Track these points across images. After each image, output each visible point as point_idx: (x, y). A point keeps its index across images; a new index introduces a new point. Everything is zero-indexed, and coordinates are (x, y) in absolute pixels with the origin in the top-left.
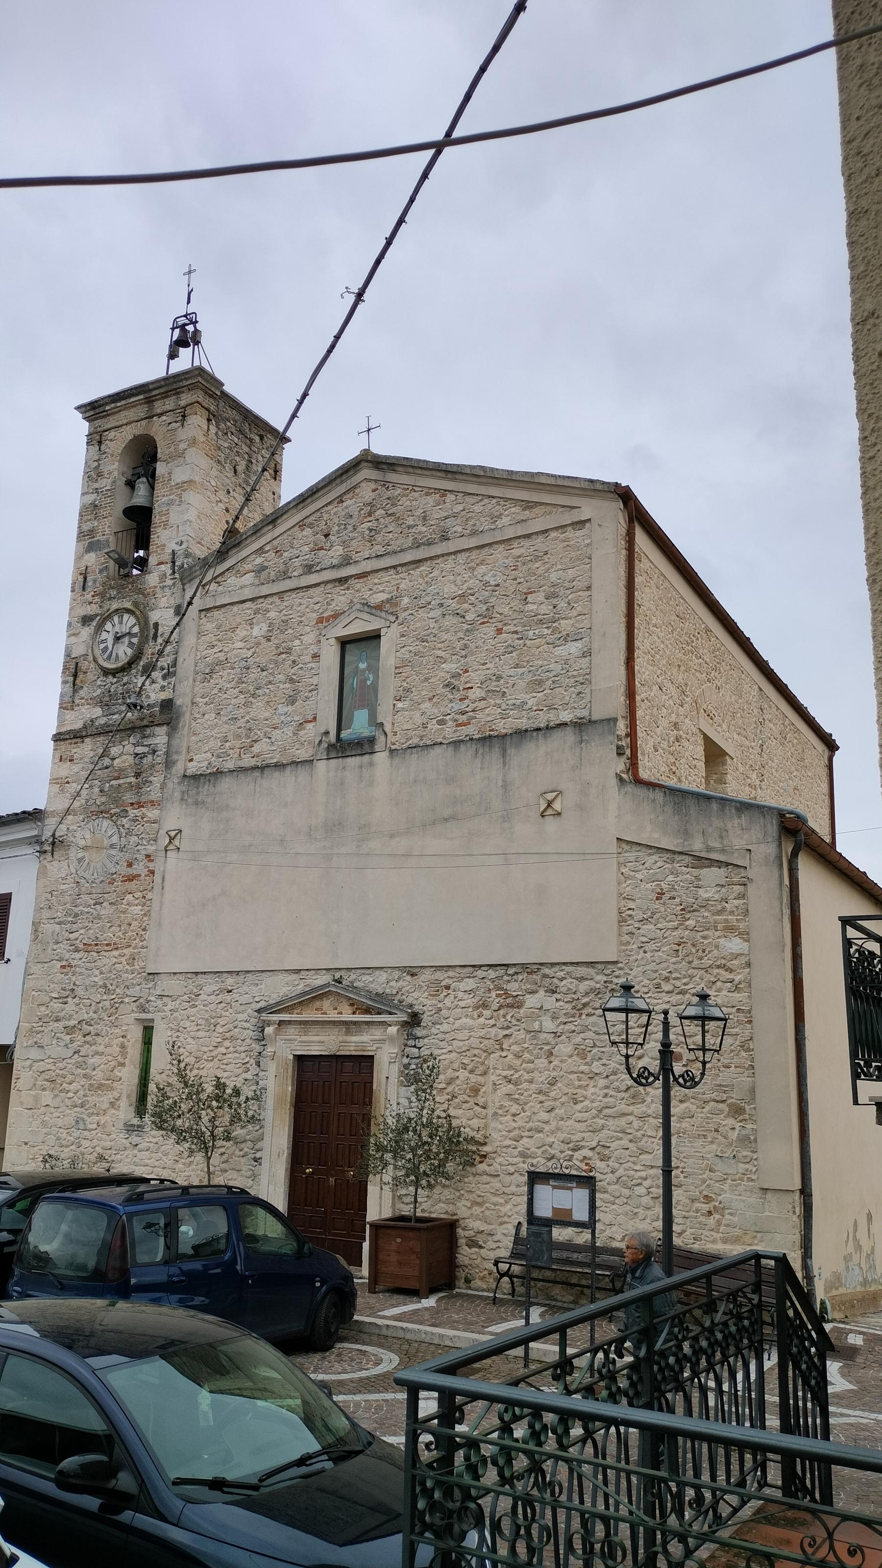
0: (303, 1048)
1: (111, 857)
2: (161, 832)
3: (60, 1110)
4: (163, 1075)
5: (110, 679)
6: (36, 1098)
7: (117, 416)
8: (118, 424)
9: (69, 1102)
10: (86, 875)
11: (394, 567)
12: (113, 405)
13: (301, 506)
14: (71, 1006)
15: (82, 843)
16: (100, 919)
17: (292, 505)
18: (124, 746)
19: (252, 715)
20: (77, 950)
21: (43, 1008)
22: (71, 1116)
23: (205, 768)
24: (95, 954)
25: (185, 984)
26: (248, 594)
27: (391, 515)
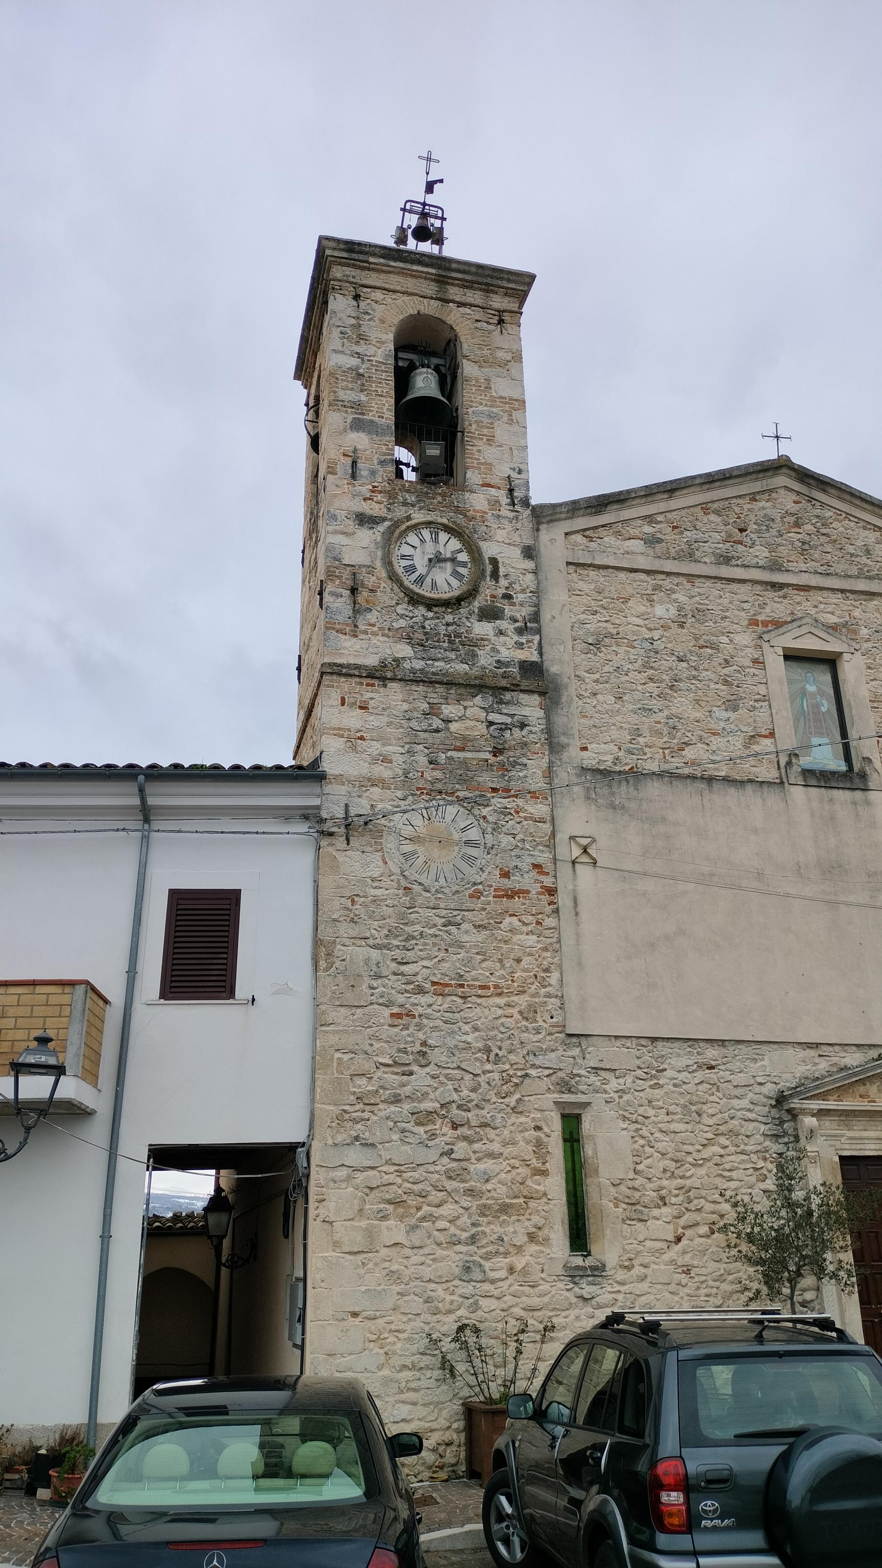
0: (854, 1147)
1: (470, 860)
2: (559, 836)
3: (426, 1251)
4: (623, 1188)
5: (422, 610)
6: (370, 1234)
7: (382, 276)
8: (387, 286)
9: (441, 1237)
10: (423, 879)
11: (842, 591)
12: (382, 261)
13: (707, 486)
14: (421, 1077)
15: (408, 831)
16: (461, 947)
17: (698, 481)
18: (465, 708)
19: (674, 710)
20: (421, 991)
21: (363, 1081)
22: (451, 1260)
23: (609, 763)
24: (460, 1000)
25: (638, 1053)
26: (642, 562)
27: (824, 534)
